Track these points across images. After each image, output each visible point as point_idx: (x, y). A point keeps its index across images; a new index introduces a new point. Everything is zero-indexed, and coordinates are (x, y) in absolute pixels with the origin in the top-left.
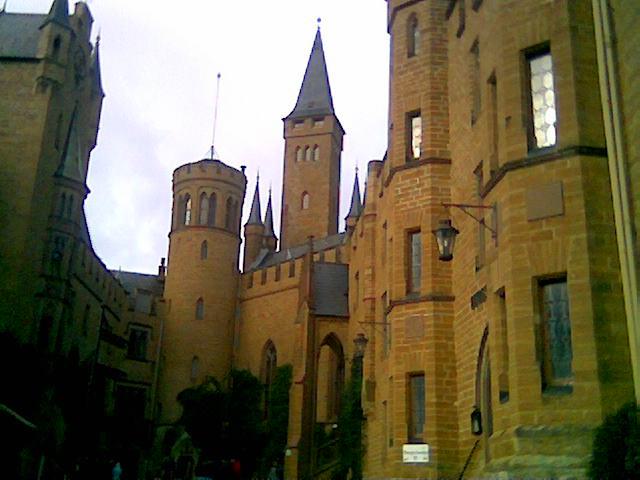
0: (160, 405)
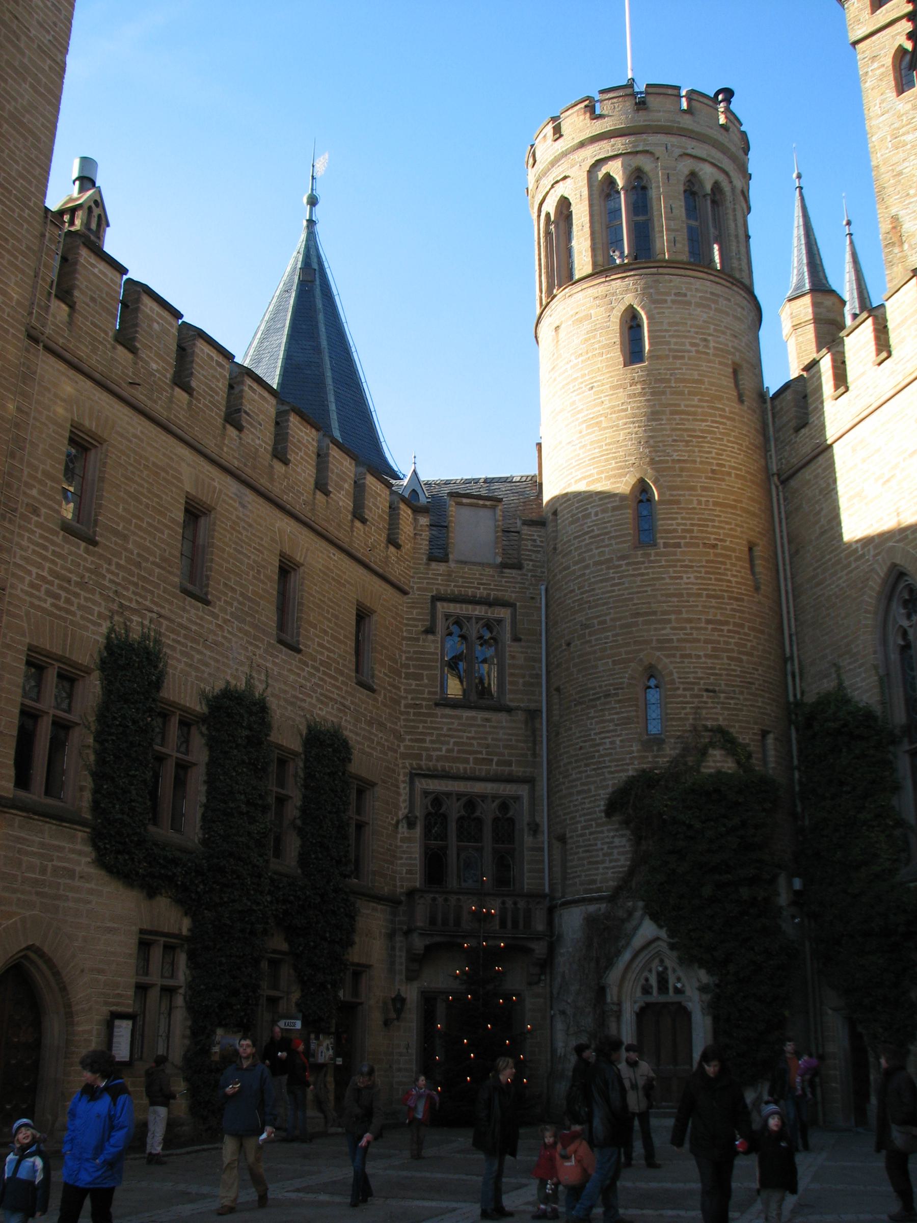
0: (562, 839)
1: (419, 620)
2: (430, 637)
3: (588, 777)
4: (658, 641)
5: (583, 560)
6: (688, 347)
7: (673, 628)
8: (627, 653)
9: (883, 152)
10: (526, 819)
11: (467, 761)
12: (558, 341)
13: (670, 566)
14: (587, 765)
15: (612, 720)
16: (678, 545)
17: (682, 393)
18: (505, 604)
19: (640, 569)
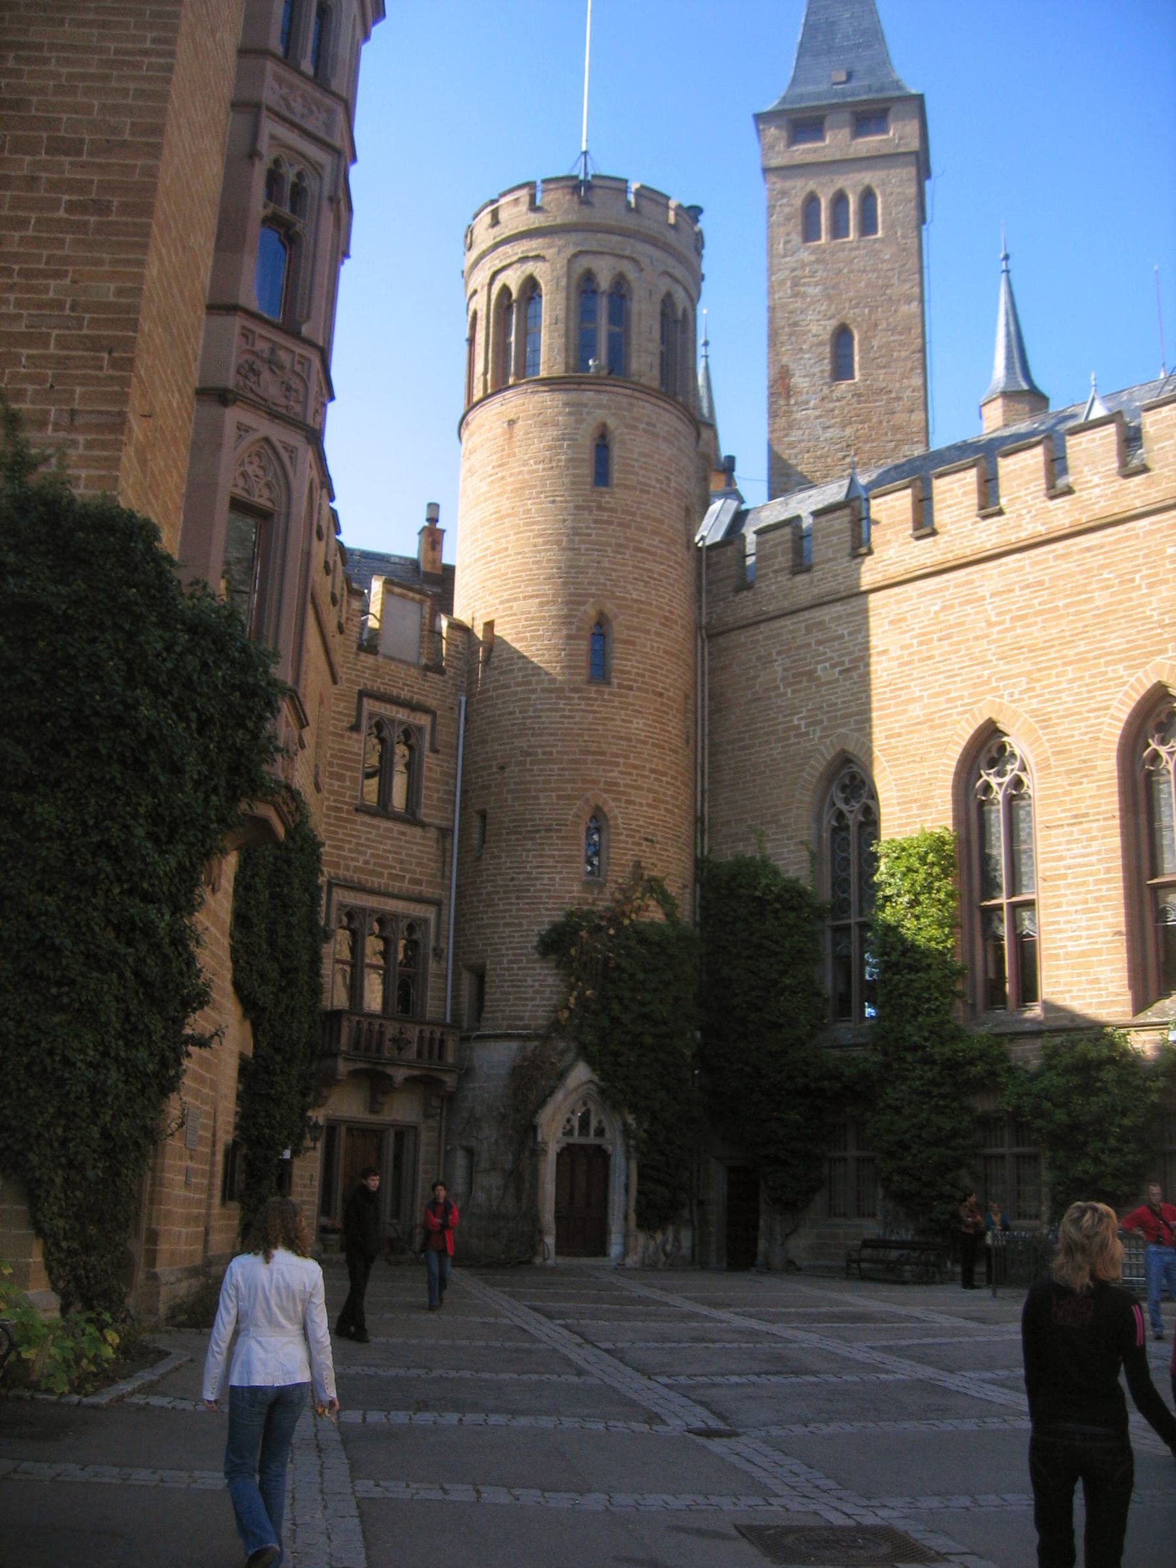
1: (345, 715)
2: (355, 735)
3: (519, 910)
4: (606, 783)
5: (529, 683)
6: (653, 482)
7: (621, 773)
8: (573, 789)
9: (781, 294)
10: (432, 944)
11: (381, 875)
12: (510, 438)
13: (622, 708)
14: (518, 898)
15: (553, 856)
16: (630, 688)
17: (644, 530)
18: (427, 711)
19: (592, 705)
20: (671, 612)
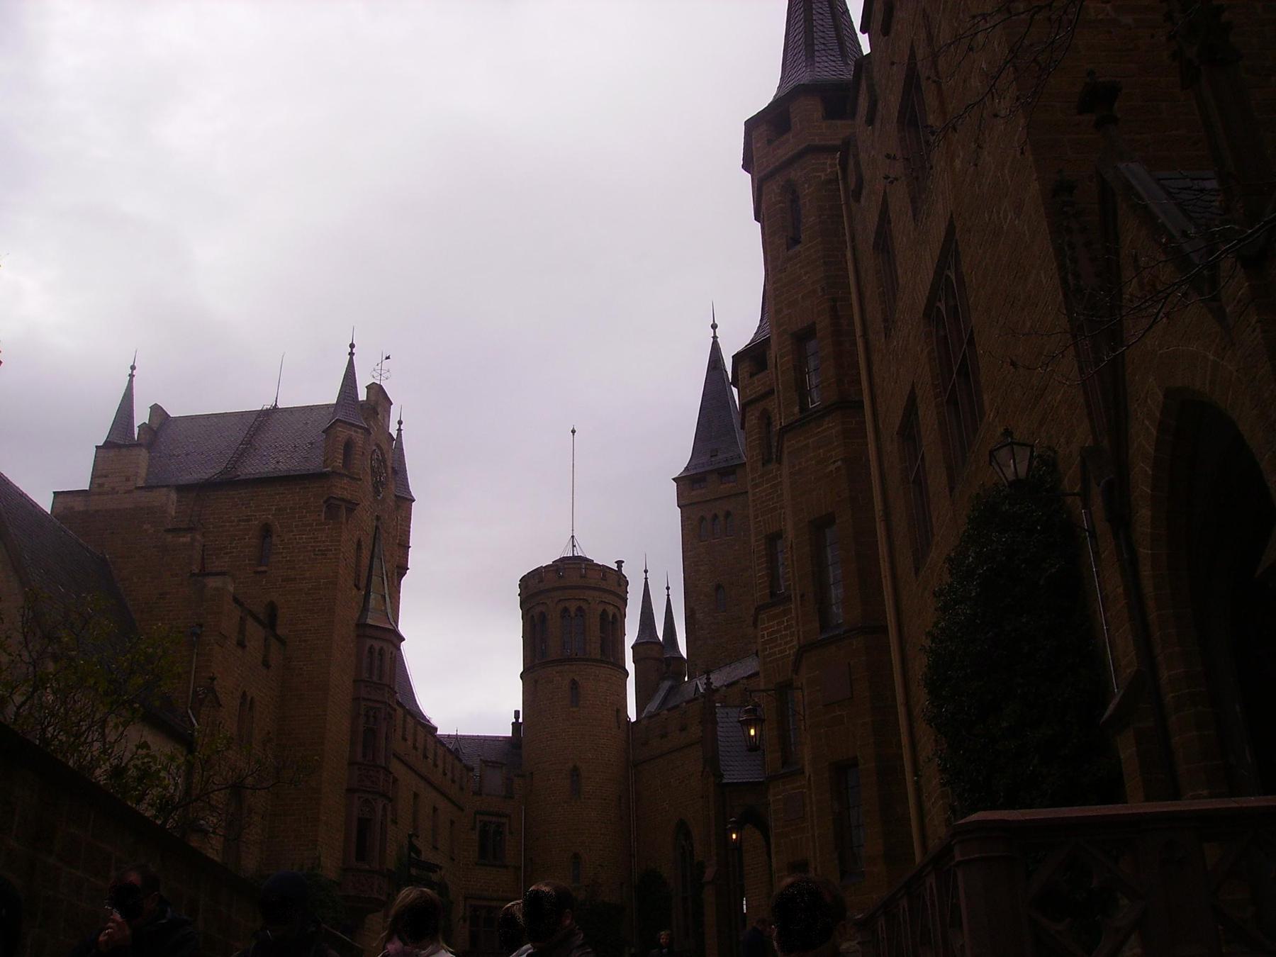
20: (609, 760)
